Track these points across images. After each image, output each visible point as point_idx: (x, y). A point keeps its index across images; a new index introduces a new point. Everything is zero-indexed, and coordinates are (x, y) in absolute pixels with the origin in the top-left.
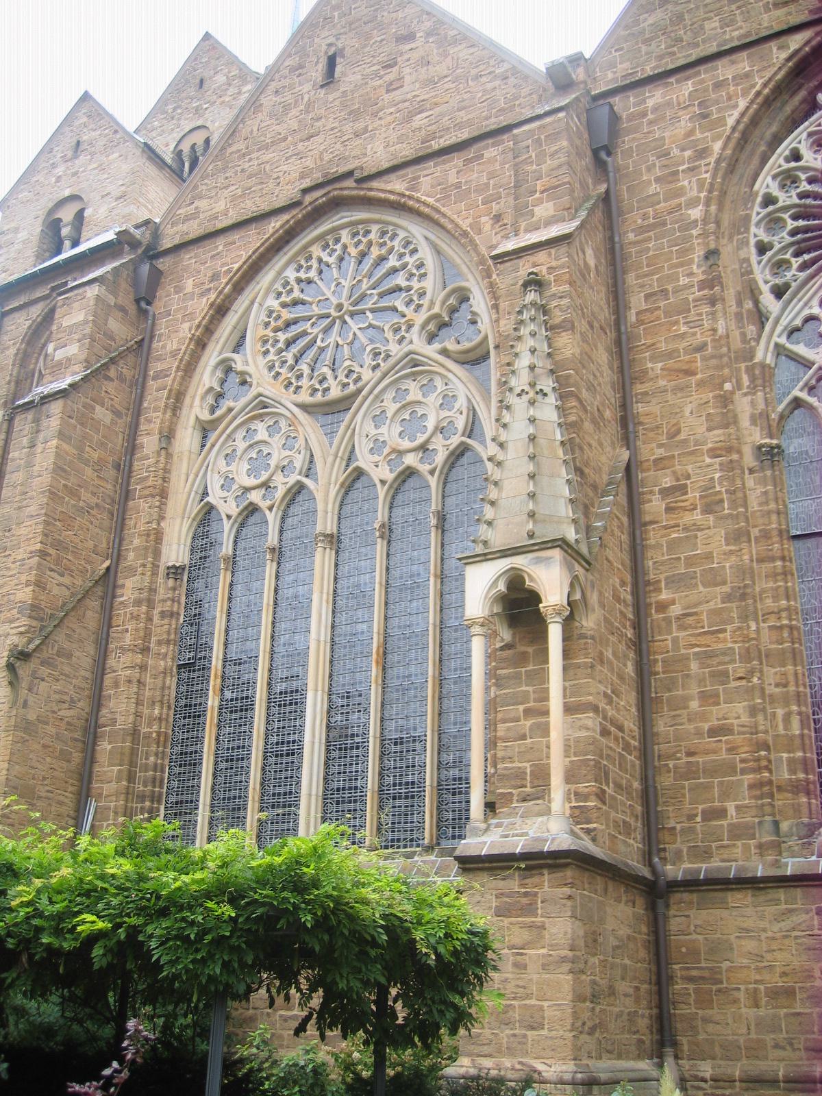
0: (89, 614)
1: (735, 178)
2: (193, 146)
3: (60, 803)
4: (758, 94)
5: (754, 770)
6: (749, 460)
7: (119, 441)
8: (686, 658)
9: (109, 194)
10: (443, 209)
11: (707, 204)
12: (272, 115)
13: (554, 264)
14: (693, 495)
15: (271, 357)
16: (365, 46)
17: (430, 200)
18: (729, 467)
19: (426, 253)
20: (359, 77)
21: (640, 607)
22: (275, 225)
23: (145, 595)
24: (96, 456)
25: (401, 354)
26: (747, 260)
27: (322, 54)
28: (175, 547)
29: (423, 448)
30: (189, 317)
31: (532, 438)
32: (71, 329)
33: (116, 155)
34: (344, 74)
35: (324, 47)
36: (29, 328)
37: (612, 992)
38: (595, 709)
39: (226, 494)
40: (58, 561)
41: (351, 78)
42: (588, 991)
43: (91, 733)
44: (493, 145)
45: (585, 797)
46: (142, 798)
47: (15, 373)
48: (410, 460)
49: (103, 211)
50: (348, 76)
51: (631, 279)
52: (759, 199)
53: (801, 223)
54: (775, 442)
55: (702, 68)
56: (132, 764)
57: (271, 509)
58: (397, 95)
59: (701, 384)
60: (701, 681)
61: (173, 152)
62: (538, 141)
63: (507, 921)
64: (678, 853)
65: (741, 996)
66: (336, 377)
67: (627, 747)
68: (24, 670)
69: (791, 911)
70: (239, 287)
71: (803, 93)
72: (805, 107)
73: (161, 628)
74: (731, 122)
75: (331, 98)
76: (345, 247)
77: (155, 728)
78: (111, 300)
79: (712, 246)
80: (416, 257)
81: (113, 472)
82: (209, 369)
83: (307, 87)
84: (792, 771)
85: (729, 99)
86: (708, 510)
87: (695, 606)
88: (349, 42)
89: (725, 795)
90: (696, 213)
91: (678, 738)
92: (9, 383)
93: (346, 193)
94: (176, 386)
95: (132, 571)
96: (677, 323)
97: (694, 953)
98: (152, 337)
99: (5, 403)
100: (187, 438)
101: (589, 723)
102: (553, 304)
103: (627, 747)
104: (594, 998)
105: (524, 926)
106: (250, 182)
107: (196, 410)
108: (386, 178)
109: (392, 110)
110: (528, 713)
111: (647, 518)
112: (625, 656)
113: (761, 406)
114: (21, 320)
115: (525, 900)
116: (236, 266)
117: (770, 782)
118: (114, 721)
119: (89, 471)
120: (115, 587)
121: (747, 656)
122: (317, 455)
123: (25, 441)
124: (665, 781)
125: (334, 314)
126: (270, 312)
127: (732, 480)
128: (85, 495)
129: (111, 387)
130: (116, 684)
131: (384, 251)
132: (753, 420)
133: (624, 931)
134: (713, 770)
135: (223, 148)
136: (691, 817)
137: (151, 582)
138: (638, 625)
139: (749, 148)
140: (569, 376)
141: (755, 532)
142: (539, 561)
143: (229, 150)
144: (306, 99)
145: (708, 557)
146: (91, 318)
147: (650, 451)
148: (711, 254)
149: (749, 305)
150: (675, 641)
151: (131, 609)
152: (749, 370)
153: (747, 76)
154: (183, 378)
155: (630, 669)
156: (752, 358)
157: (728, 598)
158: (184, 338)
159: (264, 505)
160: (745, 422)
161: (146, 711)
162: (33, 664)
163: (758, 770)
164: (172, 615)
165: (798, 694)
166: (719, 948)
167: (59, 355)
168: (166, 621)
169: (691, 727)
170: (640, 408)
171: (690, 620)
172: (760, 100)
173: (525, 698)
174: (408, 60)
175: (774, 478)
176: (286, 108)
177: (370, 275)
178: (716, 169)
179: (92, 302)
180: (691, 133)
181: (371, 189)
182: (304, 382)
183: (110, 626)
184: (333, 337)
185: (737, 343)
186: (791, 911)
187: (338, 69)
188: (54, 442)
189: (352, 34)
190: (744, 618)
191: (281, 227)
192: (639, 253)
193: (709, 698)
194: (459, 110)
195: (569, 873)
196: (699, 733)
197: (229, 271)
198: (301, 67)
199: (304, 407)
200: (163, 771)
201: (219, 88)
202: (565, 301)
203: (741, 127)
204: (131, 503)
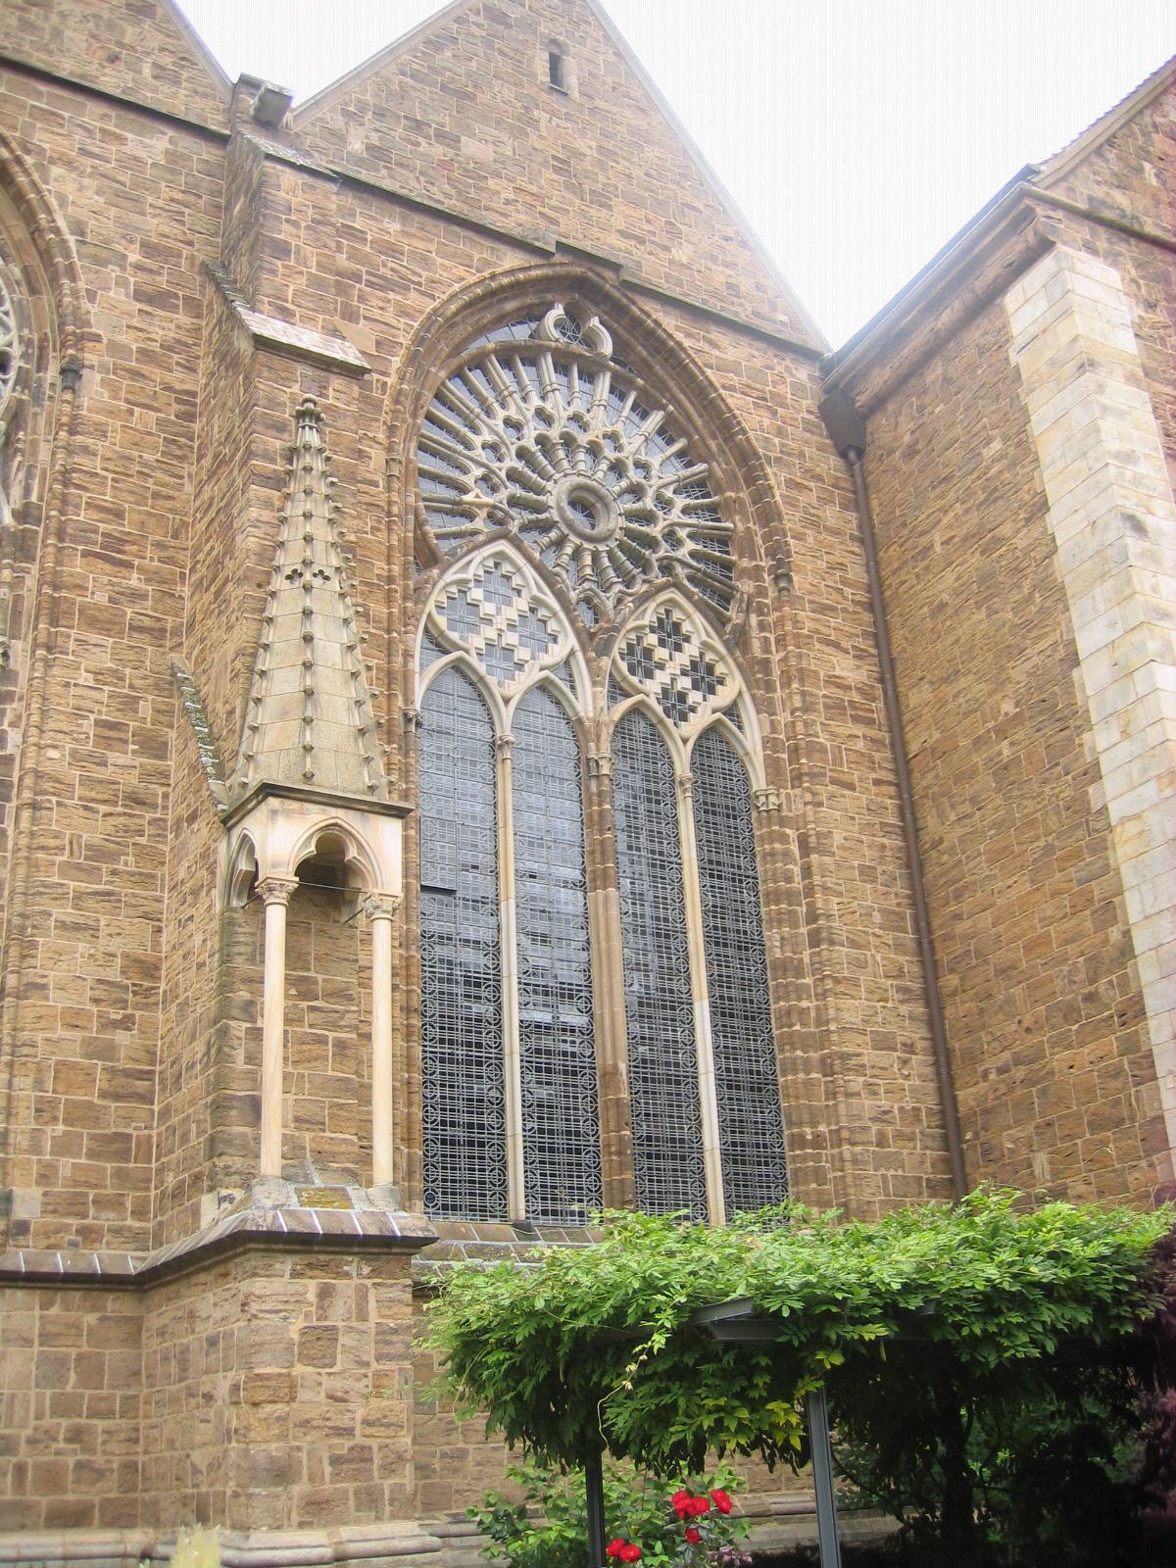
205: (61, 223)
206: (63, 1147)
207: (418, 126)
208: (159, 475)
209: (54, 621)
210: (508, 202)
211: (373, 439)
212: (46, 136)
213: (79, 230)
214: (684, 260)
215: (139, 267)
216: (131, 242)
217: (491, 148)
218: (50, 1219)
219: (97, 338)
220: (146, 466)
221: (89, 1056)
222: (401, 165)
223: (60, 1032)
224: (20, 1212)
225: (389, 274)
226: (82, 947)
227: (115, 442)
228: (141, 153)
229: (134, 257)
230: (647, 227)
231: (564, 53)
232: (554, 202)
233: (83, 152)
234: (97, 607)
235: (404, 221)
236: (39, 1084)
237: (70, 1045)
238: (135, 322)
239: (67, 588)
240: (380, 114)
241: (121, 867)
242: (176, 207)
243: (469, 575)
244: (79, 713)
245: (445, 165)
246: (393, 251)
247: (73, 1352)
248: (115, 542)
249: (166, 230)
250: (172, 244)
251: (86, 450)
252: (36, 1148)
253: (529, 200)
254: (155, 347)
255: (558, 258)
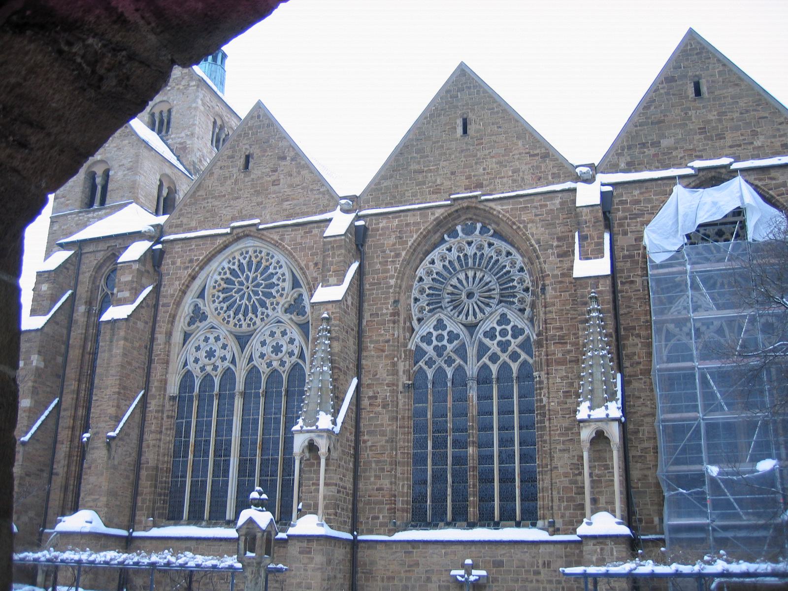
0: (136, 415)
1: (409, 267)
2: (161, 112)
3: (126, 497)
4: (421, 233)
5: (389, 504)
6: (401, 388)
7: (147, 336)
8: (370, 462)
9: (123, 165)
10: (294, 254)
11: (397, 279)
12: (218, 180)
13: (334, 311)
14: (379, 400)
15: (216, 304)
16: (263, 156)
17: (289, 248)
18: (392, 391)
19: (285, 270)
20: (260, 173)
21: (357, 441)
22: (220, 241)
23: (160, 408)
24: (138, 345)
25: (273, 316)
26: (410, 305)
27: (243, 153)
28: (173, 387)
29: (281, 360)
30: (179, 279)
31: (320, 389)
32: (126, 283)
33: (127, 142)
34: (253, 169)
35: (244, 150)
36: (97, 264)
37: (335, 577)
38: (336, 485)
39: (195, 364)
40: (125, 395)
41: (255, 172)
42: (326, 578)
43: (138, 465)
44: (318, 227)
45: (330, 515)
46: (160, 495)
47: (90, 287)
48: (275, 364)
49: (120, 174)
50: (256, 171)
51: (366, 306)
52: (417, 278)
53: (431, 292)
54: (410, 382)
55: (402, 214)
56: (156, 481)
57: (216, 376)
58: (276, 187)
59: (386, 356)
60: (375, 471)
61: (149, 113)
62: (333, 247)
63: (302, 556)
64: (363, 530)
65: (379, 578)
66: (245, 320)
67: (347, 494)
68: (113, 444)
69: (396, 552)
70: (201, 268)
71: (438, 234)
72: (440, 239)
73: (167, 423)
74: (410, 244)
75: (247, 179)
76: (251, 257)
77: (165, 466)
78: (143, 269)
79: (397, 298)
80: (281, 270)
81: (144, 350)
82: (187, 305)
83: (235, 170)
84: (403, 504)
85: (411, 232)
86: (384, 407)
87: (376, 443)
88: (256, 151)
89: (380, 511)
90: (392, 282)
91: (366, 490)
92: (87, 291)
93: (252, 234)
94: (173, 312)
95: (154, 397)
96: (381, 328)
97: (365, 564)
98: (161, 285)
99: (86, 302)
100: (177, 337)
101: (333, 490)
102: (333, 328)
103: (347, 494)
104: (329, 579)
105: (307, 558)
106: (208, 215)
107: (181, 324)
108: (270, 231)
109: (274, 196)
110: (313, 484)
111: (363, 407)
112: (350, 461)
113: (407, 367)
114: (92, 259)
115: (308, 550)
116: (201, 258)
117: (395, 508)
118: (148, 463)
119: (135, 352)
120: (147, 403)
121: (391, 464)
122: (236, 356)
123: (108, 338)
124: (360, 505)
125: (245, 290)
126: (216, 282)
127: (393, 396)
128: (135, 364)
129: (143, 311)
130: (148, 446)
131: (268, 264)
132: (404, 372)
133: (341, 557)
134: (376, 503)
135: (195, 192)
136: (368, 518)
137: (163, 403)
138: (356, 448)
139: (416, 254)
140: (335, 360)
141: (399, 416)
142: (319, 436)
143: (200, 193)
144: (235, 177)
145: (382, 425)
146: (135, 280)
147: (366, 380)
148: (396, 302)
149: (408, 324)
150: (368, 455)
151: (154, 414)
152: (405, 352)
153: (418, 223)
154: (176, 309)
155: (351, 465)
156: (407, 346)
157: (387, 441)
158: (176, 289)
159: (213, 373)
160: (401, 373)
161: (161, 458)
162: (116, 441)
163: (391, 504)
164: (172, 417)
165: (407, 478)
166: (373, 563)
167: (120, 295)
168: (169, 420)
169: (370, 487)
170: (364, 362)
171: (374, 448)
172: (422, 236)
173: (312, 479)
174: (283, 170)
175: (408, 396)
176: (225, 178)
177: (262, 274)
178: (402, 264)
179: (136, 272)
180: (394, 245)
181: (263, 235)
182: (231, 319)
183: (145, 420)
184: (245, 301)
185: (401, 340)
186: (396, 552)
187: (251, 165)
188: (122, 342)
189: (257, 146)
190: (392, 450)
191: (222, 243)
192: (370, 295)
193: (378, 477)
194: (304, 205)
195: (322, 542)
196: (373, 489)
197: (198, 260)
198: (232, 157)
199: (231, 333)
200: (168, 484)
201: (176, 78)
202: (337, 328)
203: (413, 247)
204: (153, 365)
205: (533, 242)
206: (566, 508)
207: (643, 145)
208: (571, 312)
209: (548, 366)
210: (681, 158)
211: (637, 275)
212: (525, 216)
213: (538, 242)
214: (760, 145)
215: (557, 246)
216: (554, 239)
217: (673, 138)
218: (565, 527)
219: (549, 275)
220: (568, 310)
221: (570, 484)
222: (639, 164)
223: (563, 479)
224: (557, 526)
225: (636, 212)
226: (566, 455)
227: (558, 306)
228: (553, 207)
229: (555, 244)
230: (741, 138)
231: (700, 79)
232: (701, 148)
233: (536, 215)
234: (559, 358)
235: (640, 188)
236: (559, 493)
237: (565, 482)
238: (558, 265)
239: (551, 355)
240: (629, 148)
241: (574, 431)
242: (565, 220)
243: (680, 307)
244: (558, 391)
245: (655, 155)
246: (637, 202)
247: (573, 560)
248: (561, 337)
249: (563, 230)
250: (566, 234)
251: (550, 312)
252: (560, 509)
253: (690, 153)
254: (565, 271)
255: (701, 174)
